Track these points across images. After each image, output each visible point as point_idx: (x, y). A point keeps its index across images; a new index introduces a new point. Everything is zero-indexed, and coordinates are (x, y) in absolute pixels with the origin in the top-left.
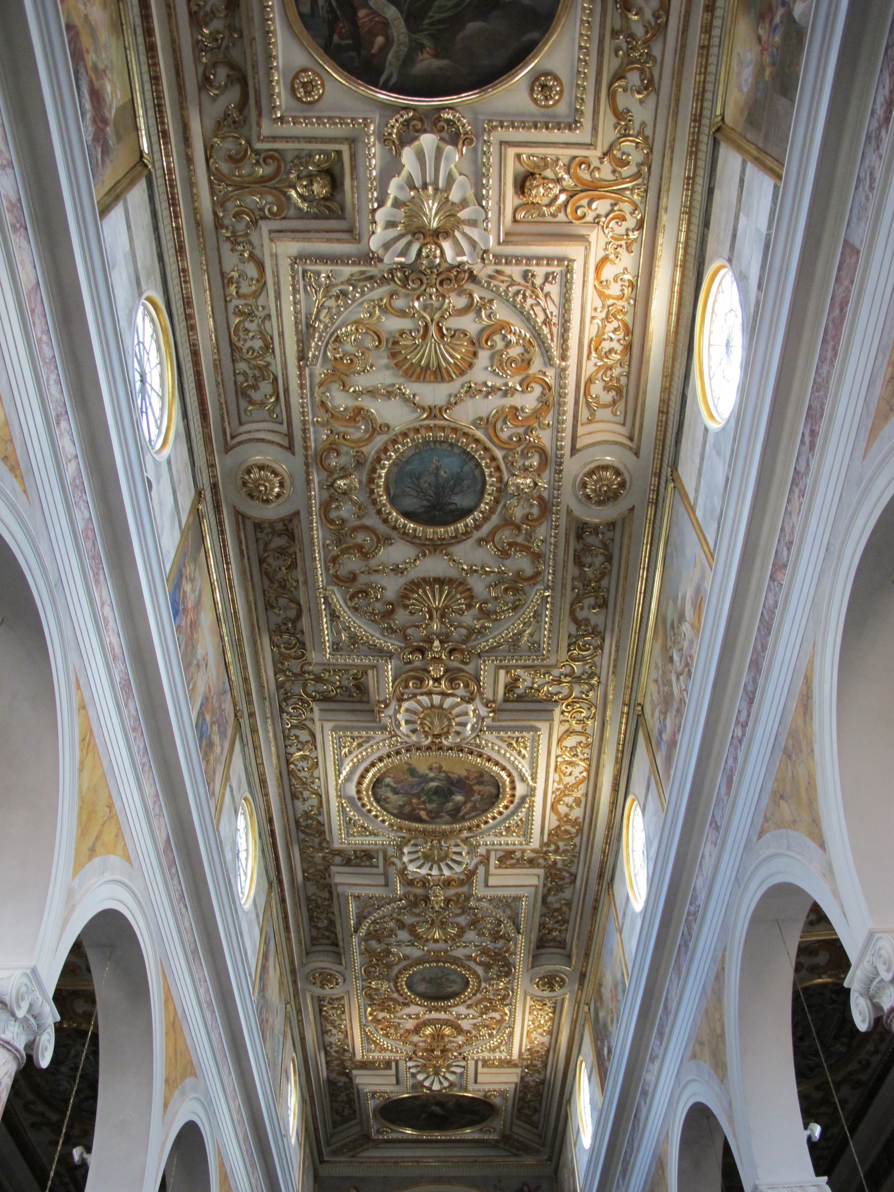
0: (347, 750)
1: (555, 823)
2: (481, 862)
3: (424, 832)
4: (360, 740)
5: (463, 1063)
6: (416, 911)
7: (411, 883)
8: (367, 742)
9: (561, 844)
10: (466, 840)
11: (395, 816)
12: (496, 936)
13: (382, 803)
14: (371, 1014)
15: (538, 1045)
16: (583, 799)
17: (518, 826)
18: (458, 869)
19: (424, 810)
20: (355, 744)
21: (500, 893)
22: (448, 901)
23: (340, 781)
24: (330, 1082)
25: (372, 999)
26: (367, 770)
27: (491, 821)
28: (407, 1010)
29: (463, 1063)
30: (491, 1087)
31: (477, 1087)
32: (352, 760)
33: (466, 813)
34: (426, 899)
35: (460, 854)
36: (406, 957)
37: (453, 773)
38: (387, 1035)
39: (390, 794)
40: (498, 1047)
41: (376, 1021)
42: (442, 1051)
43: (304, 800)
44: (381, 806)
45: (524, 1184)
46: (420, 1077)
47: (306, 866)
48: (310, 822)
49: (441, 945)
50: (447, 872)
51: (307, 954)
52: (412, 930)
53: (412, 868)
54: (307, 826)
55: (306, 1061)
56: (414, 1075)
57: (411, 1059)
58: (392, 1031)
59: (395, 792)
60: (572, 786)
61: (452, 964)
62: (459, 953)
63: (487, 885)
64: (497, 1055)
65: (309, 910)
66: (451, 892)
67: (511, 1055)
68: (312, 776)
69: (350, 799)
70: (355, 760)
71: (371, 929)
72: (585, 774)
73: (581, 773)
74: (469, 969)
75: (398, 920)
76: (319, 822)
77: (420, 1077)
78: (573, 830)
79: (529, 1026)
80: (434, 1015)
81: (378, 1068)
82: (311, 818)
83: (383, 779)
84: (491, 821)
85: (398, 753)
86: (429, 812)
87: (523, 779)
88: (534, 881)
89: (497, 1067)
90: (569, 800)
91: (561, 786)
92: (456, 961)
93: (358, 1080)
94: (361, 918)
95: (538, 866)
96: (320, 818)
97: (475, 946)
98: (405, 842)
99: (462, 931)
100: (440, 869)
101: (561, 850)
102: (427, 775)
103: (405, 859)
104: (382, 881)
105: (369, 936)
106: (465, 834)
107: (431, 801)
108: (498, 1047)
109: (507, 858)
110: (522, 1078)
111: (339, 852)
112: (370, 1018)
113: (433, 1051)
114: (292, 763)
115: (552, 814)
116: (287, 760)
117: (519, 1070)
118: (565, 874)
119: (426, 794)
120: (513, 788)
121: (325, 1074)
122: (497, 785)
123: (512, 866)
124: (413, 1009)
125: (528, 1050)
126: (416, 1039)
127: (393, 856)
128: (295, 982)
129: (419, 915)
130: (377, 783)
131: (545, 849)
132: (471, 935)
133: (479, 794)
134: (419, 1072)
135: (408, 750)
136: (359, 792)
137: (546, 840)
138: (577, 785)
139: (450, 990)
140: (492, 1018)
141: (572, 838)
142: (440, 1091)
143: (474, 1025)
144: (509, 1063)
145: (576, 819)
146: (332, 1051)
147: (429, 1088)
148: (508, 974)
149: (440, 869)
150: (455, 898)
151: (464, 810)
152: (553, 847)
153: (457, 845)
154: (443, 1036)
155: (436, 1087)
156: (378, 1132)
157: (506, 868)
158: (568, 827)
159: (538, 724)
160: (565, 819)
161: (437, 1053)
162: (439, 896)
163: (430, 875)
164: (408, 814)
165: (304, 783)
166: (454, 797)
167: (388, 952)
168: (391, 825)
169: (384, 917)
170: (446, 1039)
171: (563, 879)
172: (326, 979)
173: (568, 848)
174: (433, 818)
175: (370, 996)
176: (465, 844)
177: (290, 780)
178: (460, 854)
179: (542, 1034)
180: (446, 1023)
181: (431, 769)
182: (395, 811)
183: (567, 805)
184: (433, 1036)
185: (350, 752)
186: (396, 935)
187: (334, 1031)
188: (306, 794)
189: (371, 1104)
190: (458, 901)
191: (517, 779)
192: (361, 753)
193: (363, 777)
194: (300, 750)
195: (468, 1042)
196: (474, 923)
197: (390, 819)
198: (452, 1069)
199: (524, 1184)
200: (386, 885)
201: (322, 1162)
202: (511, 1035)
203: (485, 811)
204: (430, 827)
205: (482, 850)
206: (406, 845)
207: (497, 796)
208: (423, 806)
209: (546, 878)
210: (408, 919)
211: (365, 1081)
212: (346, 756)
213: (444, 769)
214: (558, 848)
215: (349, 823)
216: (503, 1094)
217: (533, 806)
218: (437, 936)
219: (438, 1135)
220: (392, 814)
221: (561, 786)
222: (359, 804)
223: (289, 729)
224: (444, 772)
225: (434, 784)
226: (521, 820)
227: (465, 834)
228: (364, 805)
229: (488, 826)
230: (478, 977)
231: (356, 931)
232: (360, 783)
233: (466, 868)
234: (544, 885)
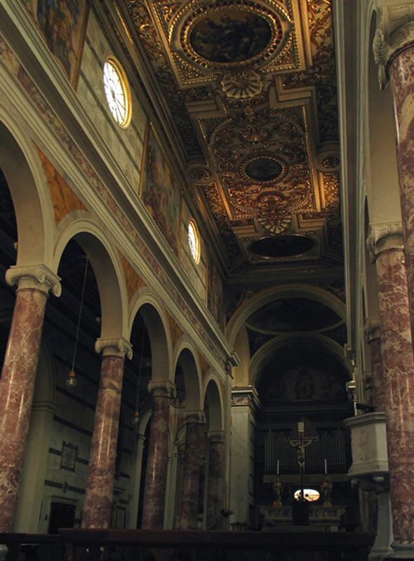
0: (167, 15)
1: (316, 51)
2: (271, 85)
3: (230, 68)
4: (173, 7)
5: (290, 217)
6: (240, 124)
7: (231, 106)
8: (178, 7)
9: (322, 66)
10: (258, 71)
11: (210, 60)
12: (293, 135)
13: (199, 52)
14: (231, 193)
15: (333, 203)
16: (331, 30)
17: (288, 55)
18: (258, 92)
19: (227, 52)
20: (171, 11)
21: (288, 105)
22: (256, 114)
23: (170, 40)
24: (222, 235)
25: (229, 184)
26: (184, 29)
27: (270, 54)
28: (251, 188)
29: (290, 217)
30: (309, 229)
31: (300, 230)
32: (172, 23)
34: (243, 116)
35: (256, 81)
36: (241, 155)
38: (243, 204)
39: (202, 44)
40: (307, 205)
41: (234, 196)
42: (276, 211)
43: (156, 59)
44: (199, 54)
46: (268, 227)
47: (171, 105)
48: (164, 74)
49: (260, 145)
50: (251, 95)
51: (187, 161)
52: (241, 139)
53: (229, 95)
54: (164, 77)
55: (204, 224)
56: (263, 226)
57: (259, 217)
58: (245, 201)
59: (205, 42)
60: (322, 20)
61: (268, 155)
62: (272, 149)
63: (278, 102)
64: (308, 210)
65: (181, 134)
66: (258, 108)
67: (314, 207)
68: (155, 41)
69: (179, 52)
70: (174, 23)
71: (217, 140)
72: (329, 9)
73: (326, 9)
74: (278, 158)
75: (231, 132)
76: (169, 73)
77: (268, 227)
78: (329, 55)
79: (325, 192)
80: (267, 190)
81: (245, 225)
82: (164, 72)
83: (195, 33)
84: (270, 54)
85: (199, 12)
87: (285, 19)
88: (309, 95)
89: (311, 218)
90: (321, 32)
91: (314, 22)
92: (270, 154)
93: (235, 232)
94: (209, 133)
95: (310, 84)
96: (169, 71)
97: (281, 143)
98: (220, 78)
99: (270, 135)
100: (247, 94)
101: (323, 71)
102: (221, 26)
103: (224, 90)
104: (214, 107)
105: (217, 145)
106: (256, 66)
108: (307, 205)
109: (290, 80)
110: (328, 224)
111: (187, 91)
112: (231, 195)
113: (270, 211)
114: (141, 33)
115: (313, 45)
116: (137, 32)
117: (324, 219)
118: (329, 88)
120: (279, 27)
121: (218, 232)
122: (266, 25)
123: (293, 87)
124: (254, 187)
125: (328, 206)
126: (260, 205)
127: (216, 89)
128: (184, 178)
129: (241, 127)
130: (192, 36)
131: (311, 71)
132: (276, 136)
134: (266, 224)
135: (205, 9)
136: (183, 46)
137: (311, 63)
138: (325, 18)
139: (272, 173)
140: (301, 188)
141: (329, 61)
142: (280, 233)
143: (291, 193)
144: (317, 216)
145: (329, 45)
146: (218, 217)
147: (274, 233)
148: (304, 159)
149: (247, 94)
150: (261, 112)
152: (317, 70)
153: (253, 75)
154: (275, 201)
155: (278, 232)
156: (253, 259)
157: (290, 88)
158: (325, 53)
160: (322, 47)
161: (273, 212)
162: (249, 112)
163: (242, 99)
164: (216, 57)
165: (152, 47)
167: (231, 154)
168: (209, 67)
169: (222, 131)
170: (277, 204)
171: (328, 91)
172: (200, 174)
173: (328, 68)
175: (227, 182)
176: (258, 73)
177: (144, 47)
178: (256, 81)
179: (333, 196)
180: (276, 194)
182: (209, 56)
183: (321, 36)
184: (269, 202)
185: (170, 17)
186: (232, 142)
187: (216, 206)
188: (156, 55)
189: (245, 245)
190: (263, 113)
191: (280, 19)
192: (176, 16)
193: (182, 34)
194: (143, 23)
195: (290, 203)
196: (276, 128)
197: (208, 64)
198: (284, 221)
200: (218, 109)
201: (228, 277)
202: (313, 197)
203: (265, 47)
204: (233, 64)
205: (269, 77)
206: (221, 80)
207: (270, 35)
209: (317, 92)
210: (239, 131)
211: (240, 232)
212: (168, 21)
213: (232, 19)
214: (320, 69)
215: (184, 70)
216: (315, 233)
217: (296, 38)
218: (256, 140)
219: (287, 259)
220: (206, 58)
221: (314, 22)
222: (186, 55)
223: (131, 8)
224: (232, 21)
226: (289, 50)
227: (256, 66)
228: (189, 55)
229: (269, 57)
230: (285, 163)
231: (208, 142)
232: (182, 39)
233: (262, 91)
234: (317, 97)
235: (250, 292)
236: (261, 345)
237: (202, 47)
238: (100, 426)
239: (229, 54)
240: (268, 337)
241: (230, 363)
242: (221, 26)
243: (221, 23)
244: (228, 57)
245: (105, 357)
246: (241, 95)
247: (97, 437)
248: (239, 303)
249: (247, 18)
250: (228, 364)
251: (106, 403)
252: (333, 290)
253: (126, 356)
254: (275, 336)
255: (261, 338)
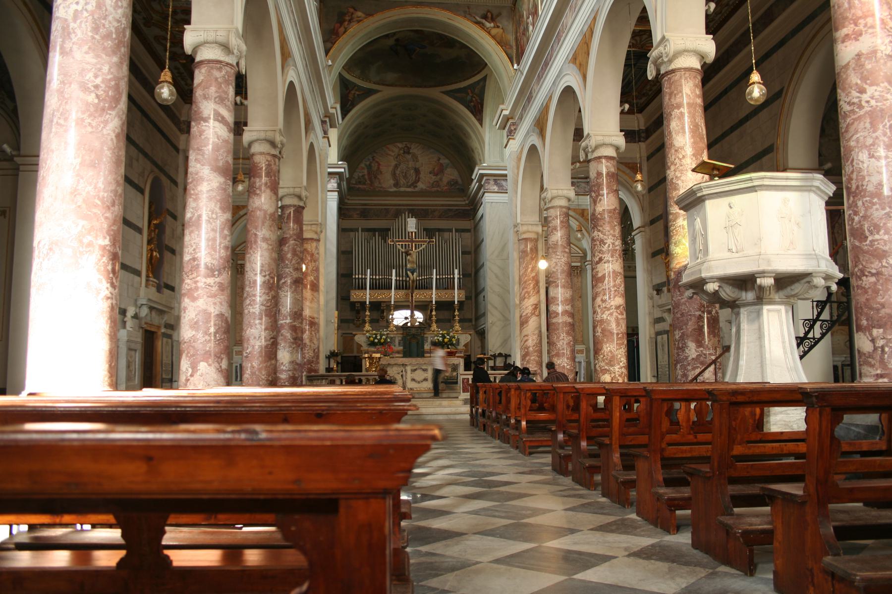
45: (488, 11)
199: (488, 11)
235: (359, 14)
236: (358, 104)
238: (199, 188)
240: (369, 92)
241: (327, 120)
245: (201, 62)
247: (196, 209)
248: (342, 30)
250: (326, 121)
251: (210, 147)
252: (483, 24)
253: (238, 64)
254: (376, 92)
255: (357, 93)
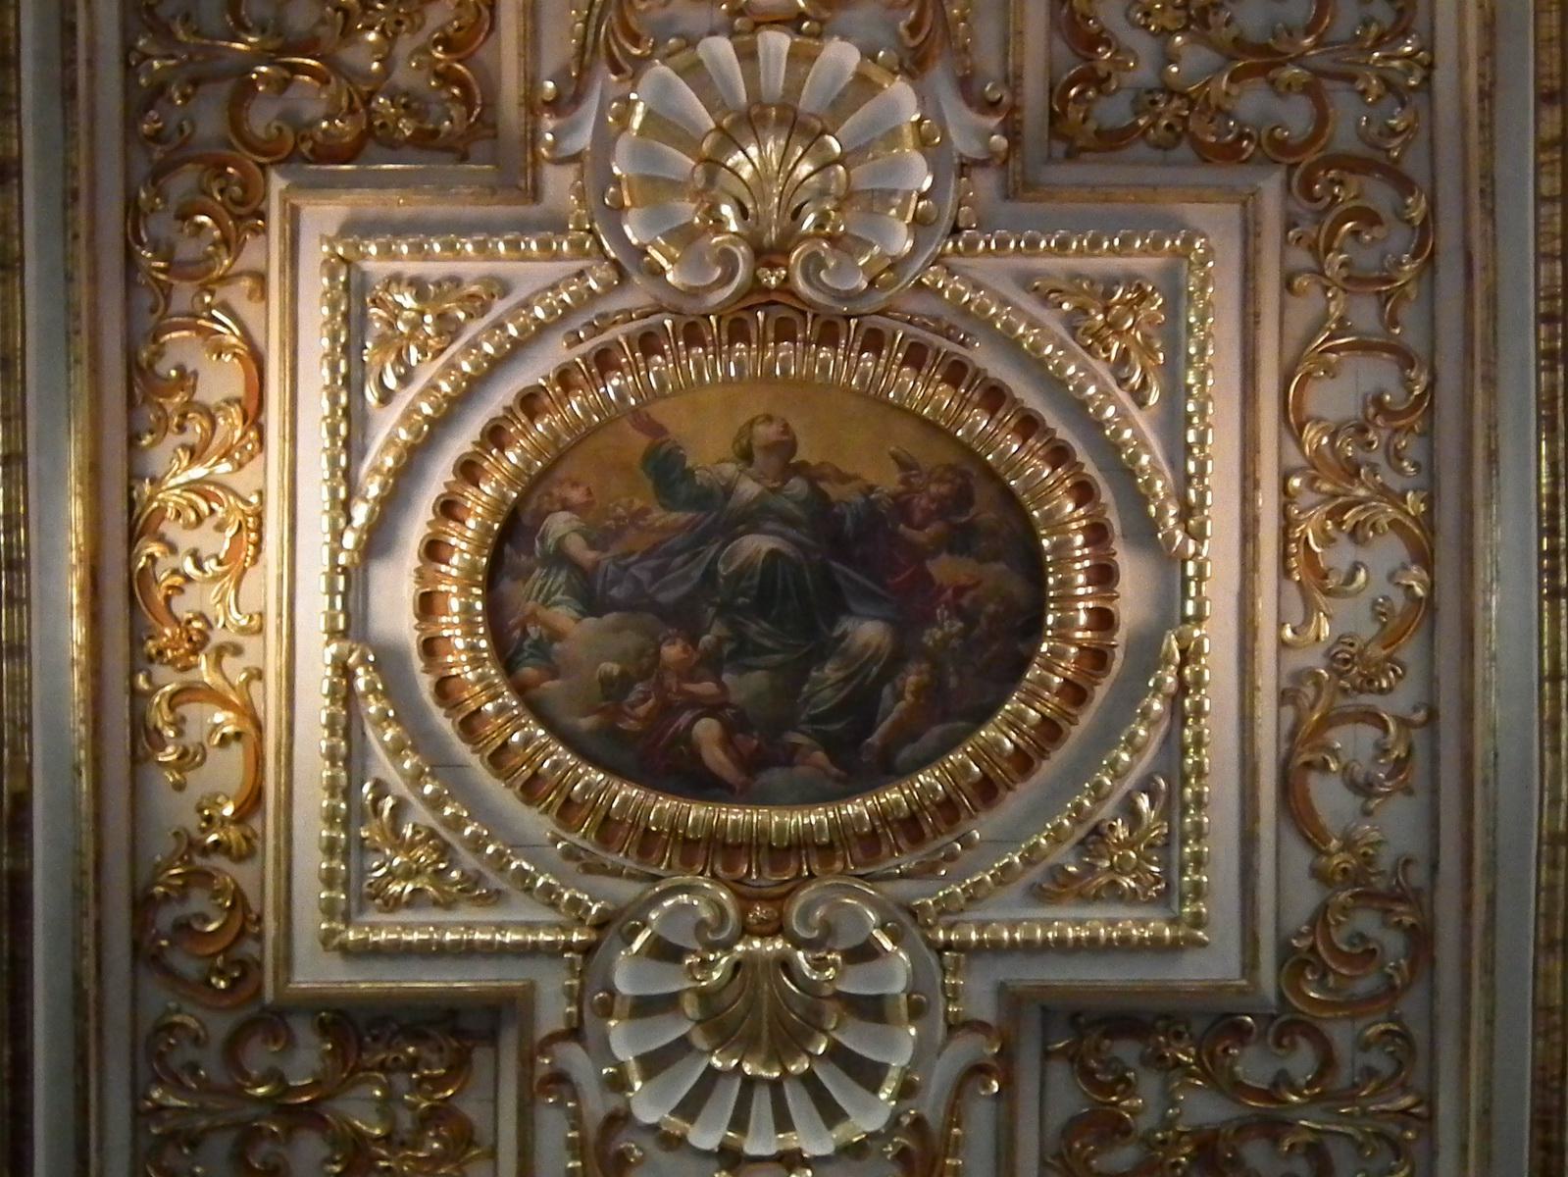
13: (528, 672)
33: (905, 732)
37: (844, 478)
39: (563, 615)
44: (520, 690)
59: (591, 601)
69: (388, 661)
83: (541, 516)
86: (734, 727)
96: (242, 875)
102: (729, 490)
107: (742, 654)
119: (723, 610)
133: (958, 612)
151: (894, 710)
159: (1194, 213)
166: (847, 624)
174: (753, 764)
181: (746, 456)
208: (707, 687)
213: (803, 454)
224: (801, 469)
225: (756, 545)
237: (557, 635)
239: (727, 741)
242: (729, 490)
243: (730, 469)
244: (715, 757)
246: (739, 1122)
249: (905, 465)
